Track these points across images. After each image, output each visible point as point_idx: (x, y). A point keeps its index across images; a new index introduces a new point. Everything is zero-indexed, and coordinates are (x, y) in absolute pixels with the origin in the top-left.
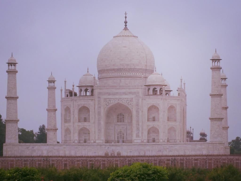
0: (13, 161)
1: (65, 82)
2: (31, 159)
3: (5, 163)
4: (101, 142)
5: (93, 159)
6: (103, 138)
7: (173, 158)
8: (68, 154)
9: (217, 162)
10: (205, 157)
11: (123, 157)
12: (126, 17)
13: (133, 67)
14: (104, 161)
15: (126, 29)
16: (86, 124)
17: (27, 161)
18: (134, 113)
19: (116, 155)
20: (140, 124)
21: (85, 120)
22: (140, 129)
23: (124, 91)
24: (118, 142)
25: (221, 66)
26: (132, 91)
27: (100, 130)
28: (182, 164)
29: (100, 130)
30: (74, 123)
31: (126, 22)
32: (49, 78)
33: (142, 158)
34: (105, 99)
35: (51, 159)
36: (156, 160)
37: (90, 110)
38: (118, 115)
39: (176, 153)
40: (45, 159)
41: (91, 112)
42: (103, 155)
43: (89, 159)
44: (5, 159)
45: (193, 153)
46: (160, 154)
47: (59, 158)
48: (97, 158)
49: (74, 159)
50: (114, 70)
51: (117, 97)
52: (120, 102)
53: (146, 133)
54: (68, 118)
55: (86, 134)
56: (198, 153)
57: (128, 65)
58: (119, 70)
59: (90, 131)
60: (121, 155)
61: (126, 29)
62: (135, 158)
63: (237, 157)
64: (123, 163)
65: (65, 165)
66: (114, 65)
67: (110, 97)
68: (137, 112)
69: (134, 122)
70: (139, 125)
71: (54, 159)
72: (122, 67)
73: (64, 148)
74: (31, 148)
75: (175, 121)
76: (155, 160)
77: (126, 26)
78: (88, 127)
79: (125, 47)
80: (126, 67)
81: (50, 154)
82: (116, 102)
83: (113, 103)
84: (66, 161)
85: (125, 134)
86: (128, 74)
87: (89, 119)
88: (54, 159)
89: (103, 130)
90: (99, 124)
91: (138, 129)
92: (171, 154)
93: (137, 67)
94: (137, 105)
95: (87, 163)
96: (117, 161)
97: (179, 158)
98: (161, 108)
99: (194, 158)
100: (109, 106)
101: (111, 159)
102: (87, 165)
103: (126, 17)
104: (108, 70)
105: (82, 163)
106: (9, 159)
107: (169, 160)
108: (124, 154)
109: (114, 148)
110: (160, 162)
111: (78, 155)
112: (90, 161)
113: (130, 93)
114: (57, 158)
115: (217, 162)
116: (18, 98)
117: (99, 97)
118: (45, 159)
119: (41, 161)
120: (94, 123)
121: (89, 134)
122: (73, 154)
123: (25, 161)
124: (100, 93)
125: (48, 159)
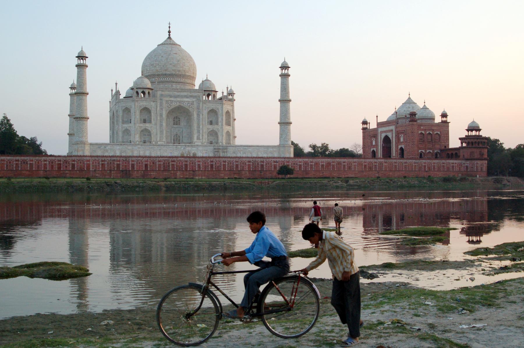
0: (89, 161)
1: (116, 84)
2: (109, 159)
3: (81, 163)
4: (163, 143)
5: (175, 159)
6: (164, 140)
7: (254, 159)
8: (142, 154)
9: (294, 164)
10: (283, 160)
11: (198, 157)
12: (169, 27)
13: (184, 74)
14: (186, 161)
15: (169, 38)
16: (147, 125)
17: (104, 161)
18: (195, 116)
19: (192, 155)
20: (201, 127)
21: (145, 121)
22: (201, 132)
23: (185, 94)
24: (174, 143)
25: (289, 73)
26: (194, 94)
27: (161, 132)
28: (262, 166)
29: (161, 132)
30: (135, 124)
31: (169, 32)
32: (71, 85)
33: (223, 159)
34: (167, 101)
35: (130, 159)
36: (238, 162)
37: (152, 112)
38: (174, 118)
39: (249, 155)
40: (124, 159)
41: (152, 114)
42: (180, 155)
43: (171, 159)
44: (80, 158)
45: (265, 155)
46: (234, 155)
47: (139, 158)
48: (179, 159)
49: (155, 159)
50: (165, 74)
51: (179, 99)
52: (182, 105)
53: (205, 136)
54: (125, 120)
55: (145, 135)
56: (270, 155)
57: (179, 71)
58: (171, 75)
59: (152, 132)
60: (197, 156)
61: (169, 38)
62: (218, 159)
63: (311, 160)
64: (205, 163)
65: (146, 165)
66: (166, 70)
67: (172, 99)
68: (198, 115)
69: (195, 125)
70: (199, 127)
71: (133, 159)
72: (174, 73)
73: (139, 148)
74: (103, 147)
75: (230, 125)
76: (236, 162)
77: (169, 35)
78: (149, 129)
79: (176, 54)
80: (177, 73)
81: (124, 154)
82: (178, 104)
83: (174, 105)
84: (147, 161)
85: (181, 137)
86: (179, 80)
87: (151, 121)
88: (133, 159)
89: (165, 132)
90: (161, 125)
91: (199, 132)
92: (244, 156)
93: (187, 74)
94: (198, 108)
95: (169, 163)
96: (200, 161)
97: (259, 160)
98: (220, 113)
99: (273, 160)
100: (171, 108)
101: (194, 159)
102: (169, 166)
103: (169, 27)
104: (158, 75)
105: (164, 164)
106: (85, 158)
107: (250, 162)
108: (200, 154)
109: (189, 148)
110: (241, 163)
111: (153, 155)
112: (172, 161)
113: (191, 96)
114: (137, 158)
115: (294, 164)
116: (88, 94)
117: (161, 99)
118: (124, 159)
119: (119, 161)
120: (156, 124)
121: (150, 135)
122: (147, 154)
123: (102, 161)
124: (162, 95)
125: (128, 159)
